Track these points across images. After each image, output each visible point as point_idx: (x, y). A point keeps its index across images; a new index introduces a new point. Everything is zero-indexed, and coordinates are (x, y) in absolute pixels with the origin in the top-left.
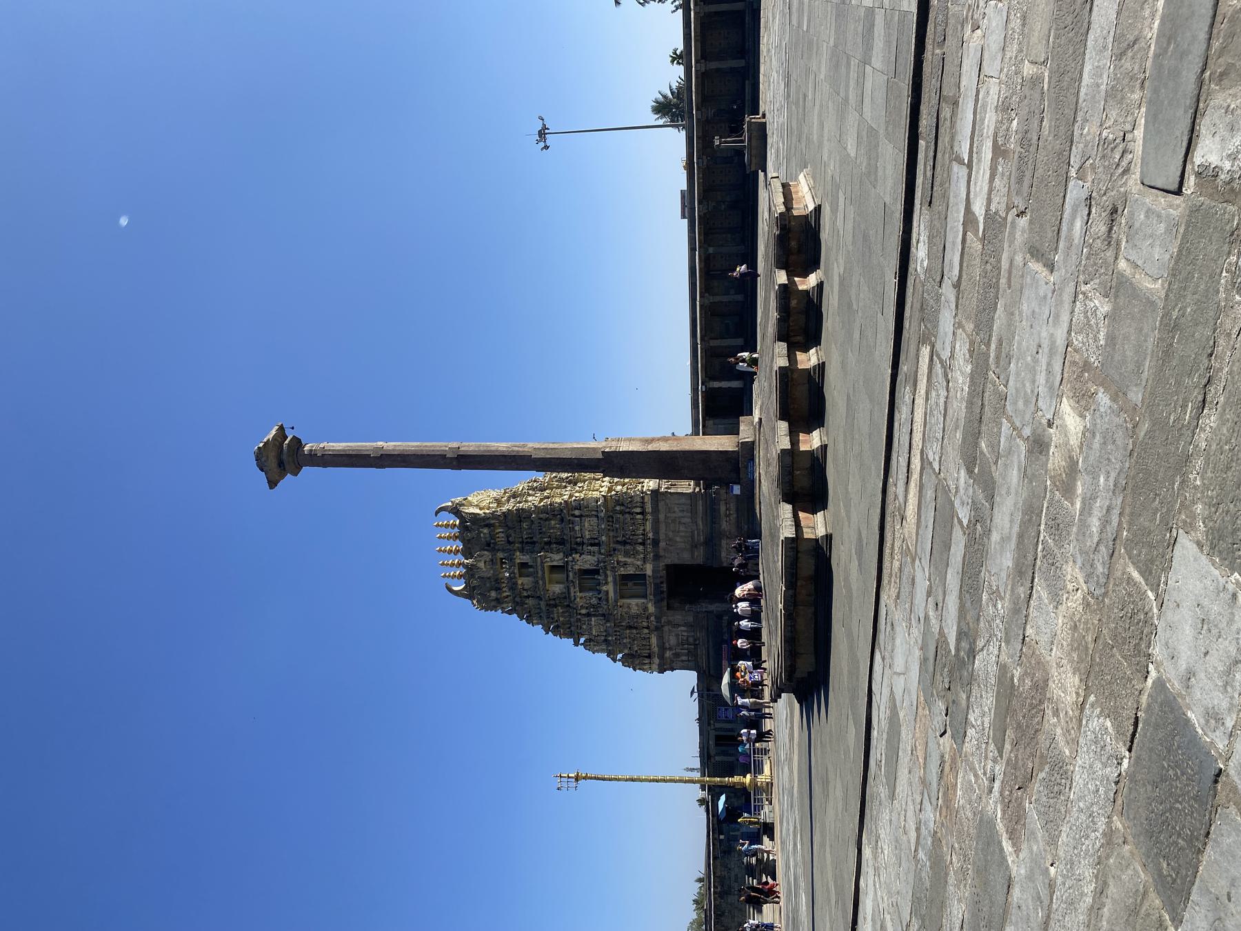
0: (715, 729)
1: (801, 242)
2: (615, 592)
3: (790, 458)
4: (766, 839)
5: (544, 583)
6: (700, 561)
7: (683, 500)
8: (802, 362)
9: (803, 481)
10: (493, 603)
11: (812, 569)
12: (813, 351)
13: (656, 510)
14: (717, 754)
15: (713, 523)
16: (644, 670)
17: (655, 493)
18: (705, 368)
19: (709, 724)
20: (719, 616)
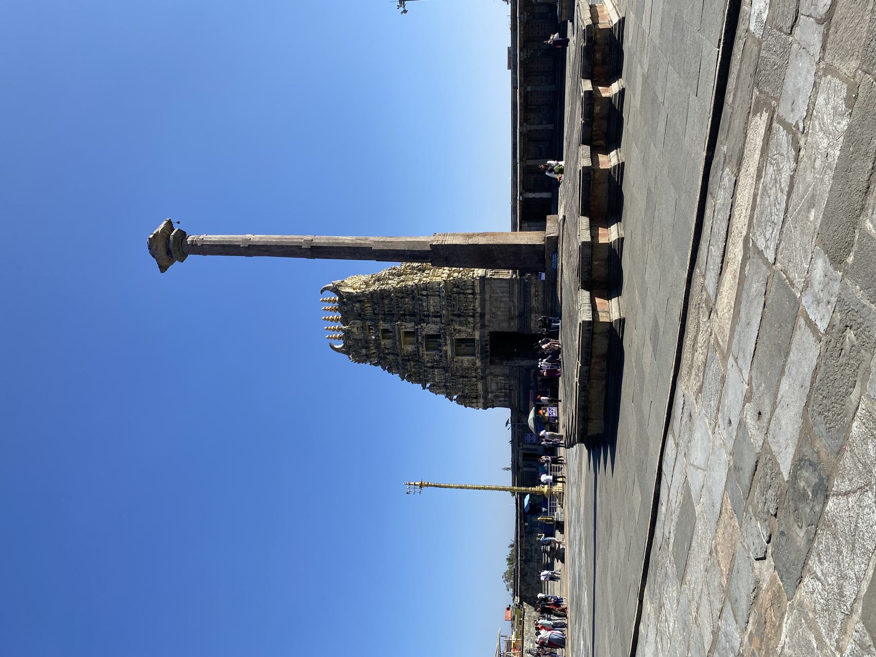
0: (523, 449)
1: (606, 53)
2: (452, 351)
3: (590, 249)
4: (557, 533)
5: (400, 344)
7: (503, 284)
8: (603, 163)
9: (600, 270)
10: (364, 358)
11: (606, 350)
12: (613, 153)
13: (483, 291)
14: (525, 466)
15: (525, 301)
17: (483, 278)
18: (522, 181)
19: (519, 445)
20: (528, 369)
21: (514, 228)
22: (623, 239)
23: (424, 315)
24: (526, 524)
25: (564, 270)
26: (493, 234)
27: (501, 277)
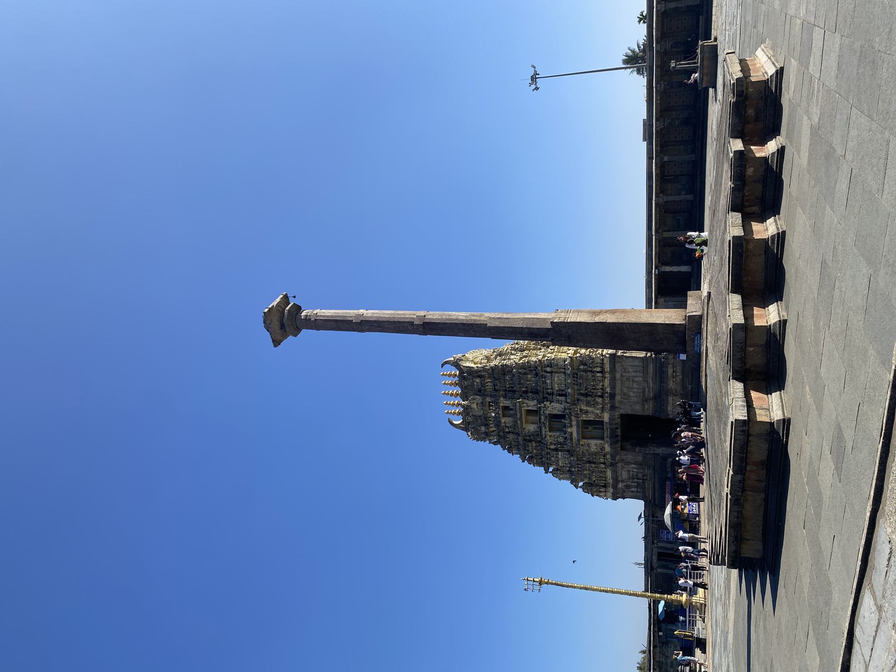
1: (760, 107)
3: (743, 334)
4: (698, 652)
5: (522, 423)
6: (649, 412)
7: (637, 363)
8: (758, 232)
9: (756, 358)
11: (765, 458)
12: (771, 220)
13: (613, 370)
14: (659, 567)
15: (661, 382)
16: (600, 496)
17: (613, 356)
19: (653, 543)
20: (665, 458)
21: (649, 306)
22: (785, 321)
23: (548, 393)
24: (661, 634)
25: (710, 355)
26: (623, 311)
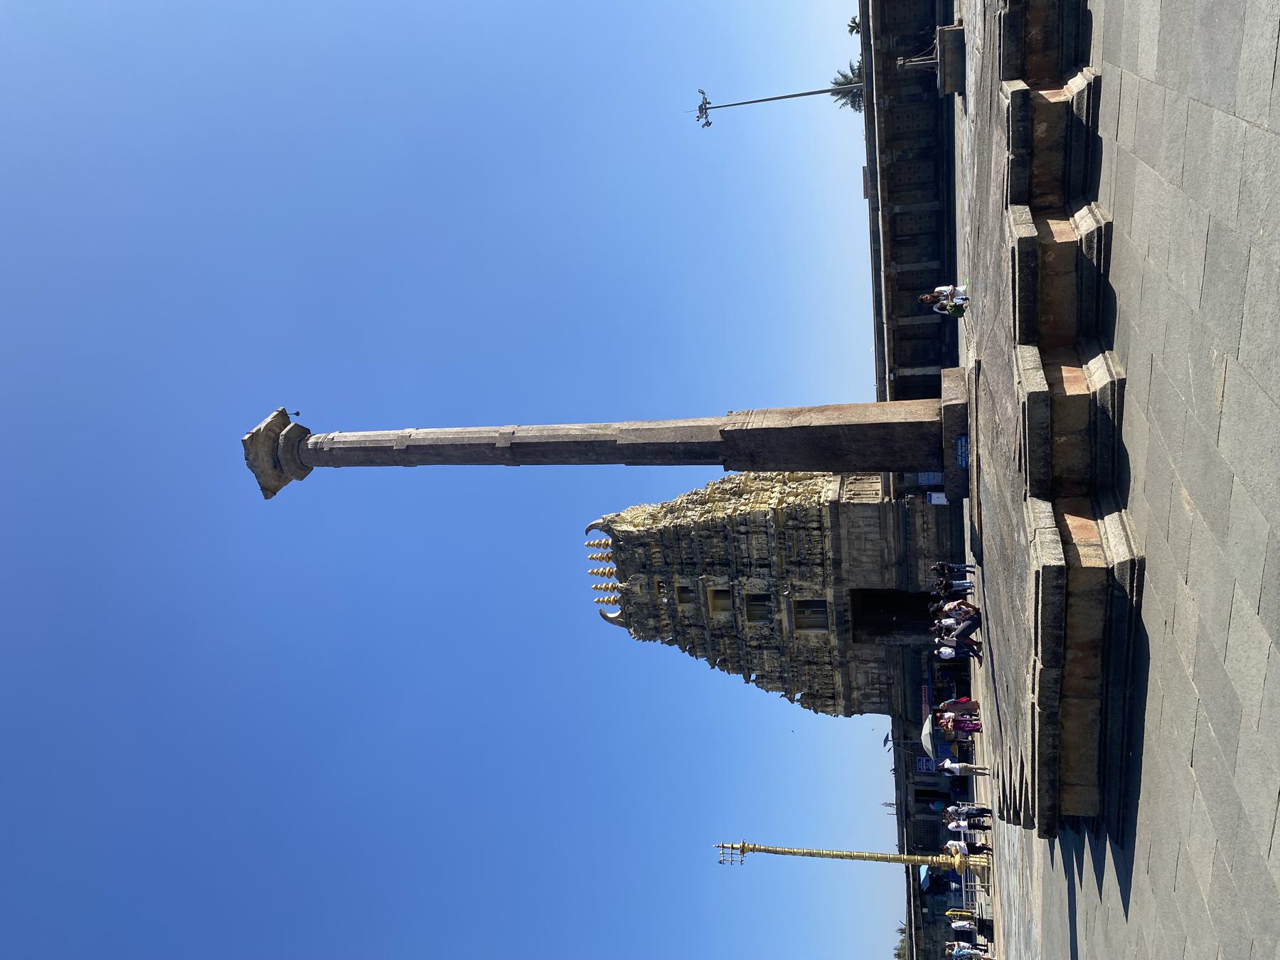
0: (915, 783)
3: (1046, 410)
6: (892, 585)
7: (869, 513)
8: (1062, 233)
9: (1072, 457)
10: (651, 633)
13: (836, 525)
14: (919, 812)
15: (906, 539)
16: (827, 713)
18: (893, 353)
19: (907, 777)
20: (917, 651)
21: (881, 397)
22: (1122, 383)
24: (925, 910)
25: (984, 467)
26: (838, 408)
27: (865, 501)
